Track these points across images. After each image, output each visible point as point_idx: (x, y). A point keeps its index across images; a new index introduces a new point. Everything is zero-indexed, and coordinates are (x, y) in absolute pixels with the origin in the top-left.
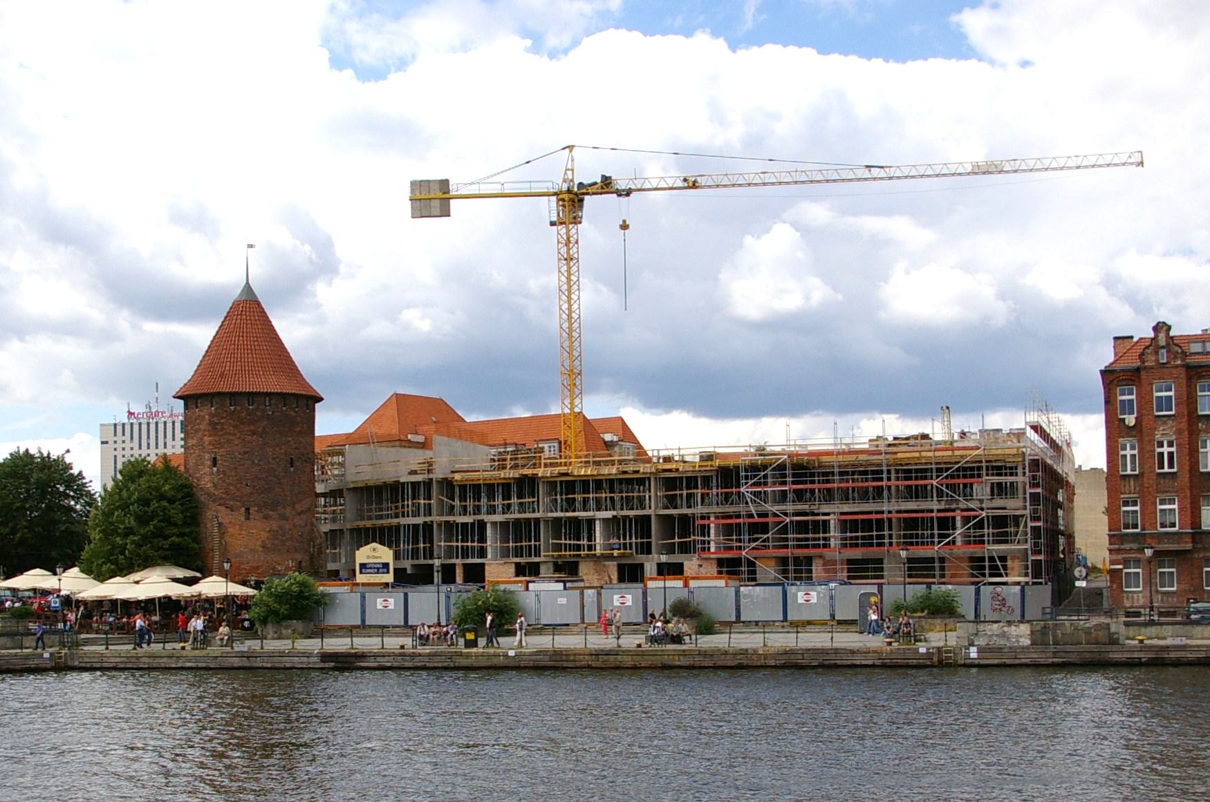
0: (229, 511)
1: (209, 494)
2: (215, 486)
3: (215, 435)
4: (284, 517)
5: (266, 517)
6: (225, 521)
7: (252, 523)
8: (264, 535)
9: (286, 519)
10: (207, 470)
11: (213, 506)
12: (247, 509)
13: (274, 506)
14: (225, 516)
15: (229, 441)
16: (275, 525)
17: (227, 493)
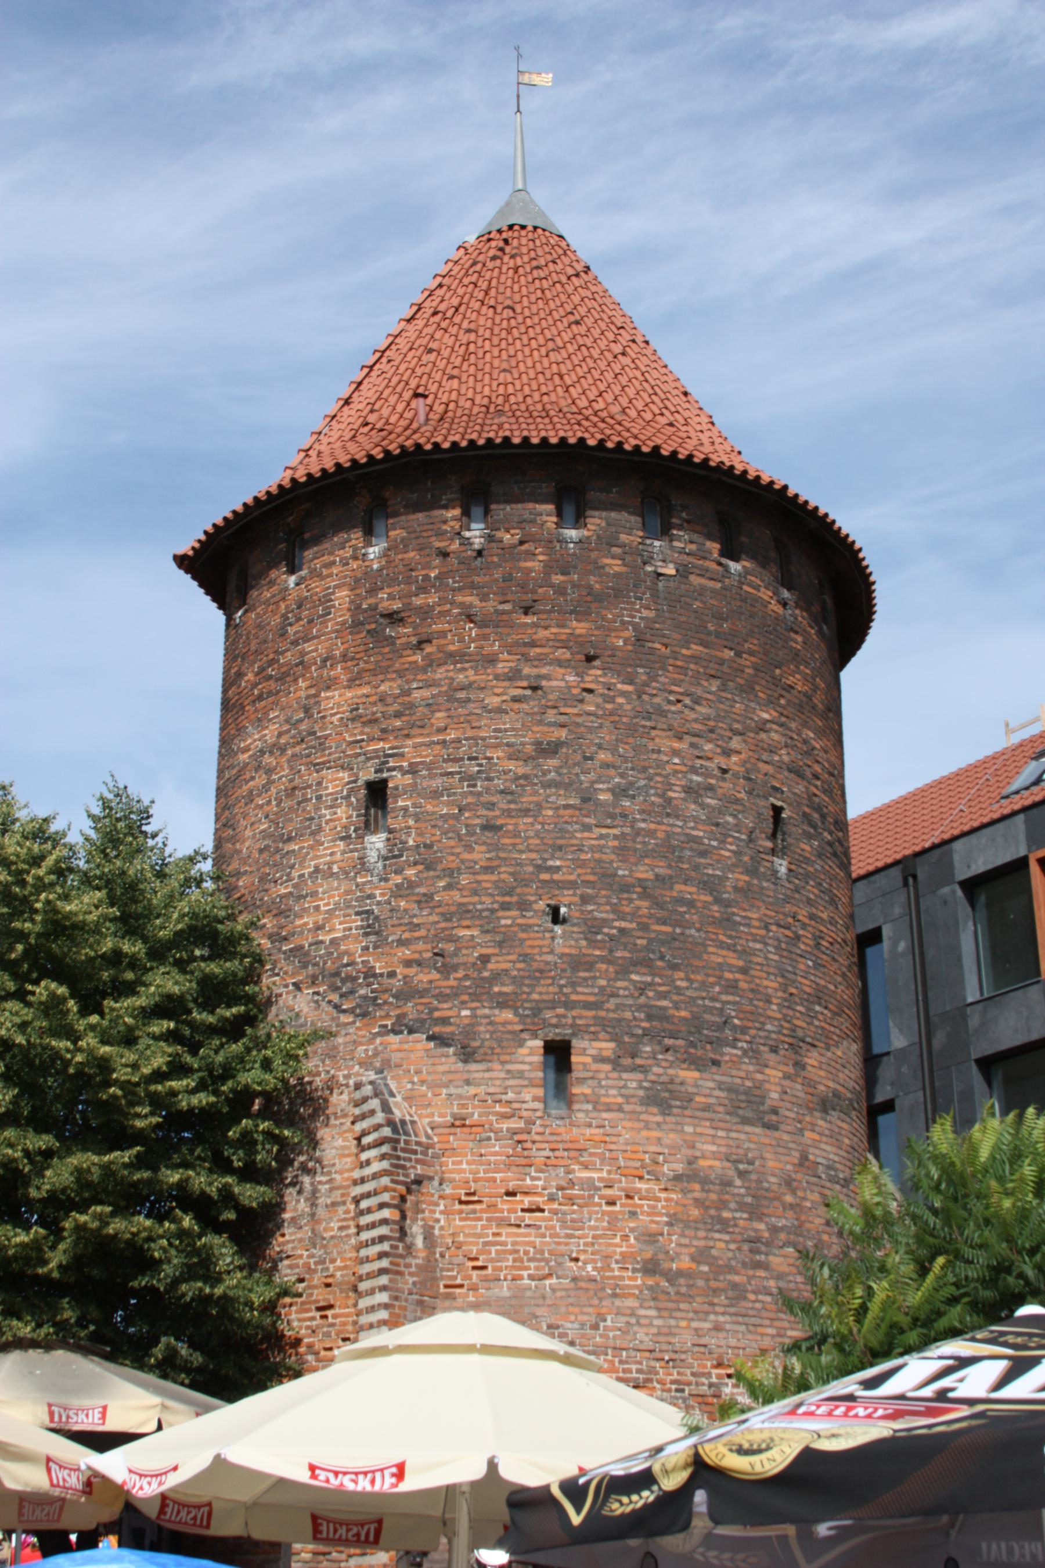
0: (448, 1060)
1: (338, 980)
2: (373, 927)
3: (380, 671)
4: (749, 1107)
5: (663, 1099)
6: (426, 1119)
7: (582, 1124)
8: (657, 1204)
9: (767, 1119)
10: (331, 851)
11: (356, 1039)
12: (559, 1054)
13: (701, 1040)
14: (424, 1087)
15: (453, 694)
16: (711, 1145)
17: (442, 961)
